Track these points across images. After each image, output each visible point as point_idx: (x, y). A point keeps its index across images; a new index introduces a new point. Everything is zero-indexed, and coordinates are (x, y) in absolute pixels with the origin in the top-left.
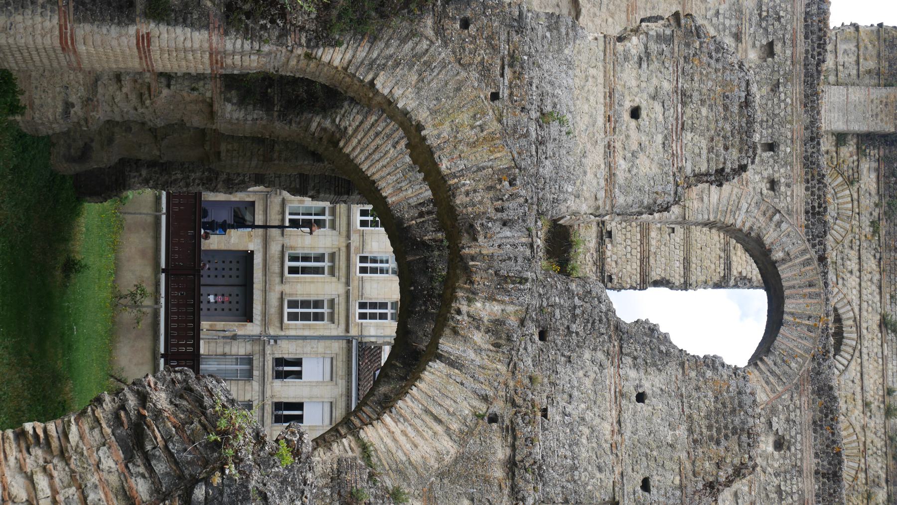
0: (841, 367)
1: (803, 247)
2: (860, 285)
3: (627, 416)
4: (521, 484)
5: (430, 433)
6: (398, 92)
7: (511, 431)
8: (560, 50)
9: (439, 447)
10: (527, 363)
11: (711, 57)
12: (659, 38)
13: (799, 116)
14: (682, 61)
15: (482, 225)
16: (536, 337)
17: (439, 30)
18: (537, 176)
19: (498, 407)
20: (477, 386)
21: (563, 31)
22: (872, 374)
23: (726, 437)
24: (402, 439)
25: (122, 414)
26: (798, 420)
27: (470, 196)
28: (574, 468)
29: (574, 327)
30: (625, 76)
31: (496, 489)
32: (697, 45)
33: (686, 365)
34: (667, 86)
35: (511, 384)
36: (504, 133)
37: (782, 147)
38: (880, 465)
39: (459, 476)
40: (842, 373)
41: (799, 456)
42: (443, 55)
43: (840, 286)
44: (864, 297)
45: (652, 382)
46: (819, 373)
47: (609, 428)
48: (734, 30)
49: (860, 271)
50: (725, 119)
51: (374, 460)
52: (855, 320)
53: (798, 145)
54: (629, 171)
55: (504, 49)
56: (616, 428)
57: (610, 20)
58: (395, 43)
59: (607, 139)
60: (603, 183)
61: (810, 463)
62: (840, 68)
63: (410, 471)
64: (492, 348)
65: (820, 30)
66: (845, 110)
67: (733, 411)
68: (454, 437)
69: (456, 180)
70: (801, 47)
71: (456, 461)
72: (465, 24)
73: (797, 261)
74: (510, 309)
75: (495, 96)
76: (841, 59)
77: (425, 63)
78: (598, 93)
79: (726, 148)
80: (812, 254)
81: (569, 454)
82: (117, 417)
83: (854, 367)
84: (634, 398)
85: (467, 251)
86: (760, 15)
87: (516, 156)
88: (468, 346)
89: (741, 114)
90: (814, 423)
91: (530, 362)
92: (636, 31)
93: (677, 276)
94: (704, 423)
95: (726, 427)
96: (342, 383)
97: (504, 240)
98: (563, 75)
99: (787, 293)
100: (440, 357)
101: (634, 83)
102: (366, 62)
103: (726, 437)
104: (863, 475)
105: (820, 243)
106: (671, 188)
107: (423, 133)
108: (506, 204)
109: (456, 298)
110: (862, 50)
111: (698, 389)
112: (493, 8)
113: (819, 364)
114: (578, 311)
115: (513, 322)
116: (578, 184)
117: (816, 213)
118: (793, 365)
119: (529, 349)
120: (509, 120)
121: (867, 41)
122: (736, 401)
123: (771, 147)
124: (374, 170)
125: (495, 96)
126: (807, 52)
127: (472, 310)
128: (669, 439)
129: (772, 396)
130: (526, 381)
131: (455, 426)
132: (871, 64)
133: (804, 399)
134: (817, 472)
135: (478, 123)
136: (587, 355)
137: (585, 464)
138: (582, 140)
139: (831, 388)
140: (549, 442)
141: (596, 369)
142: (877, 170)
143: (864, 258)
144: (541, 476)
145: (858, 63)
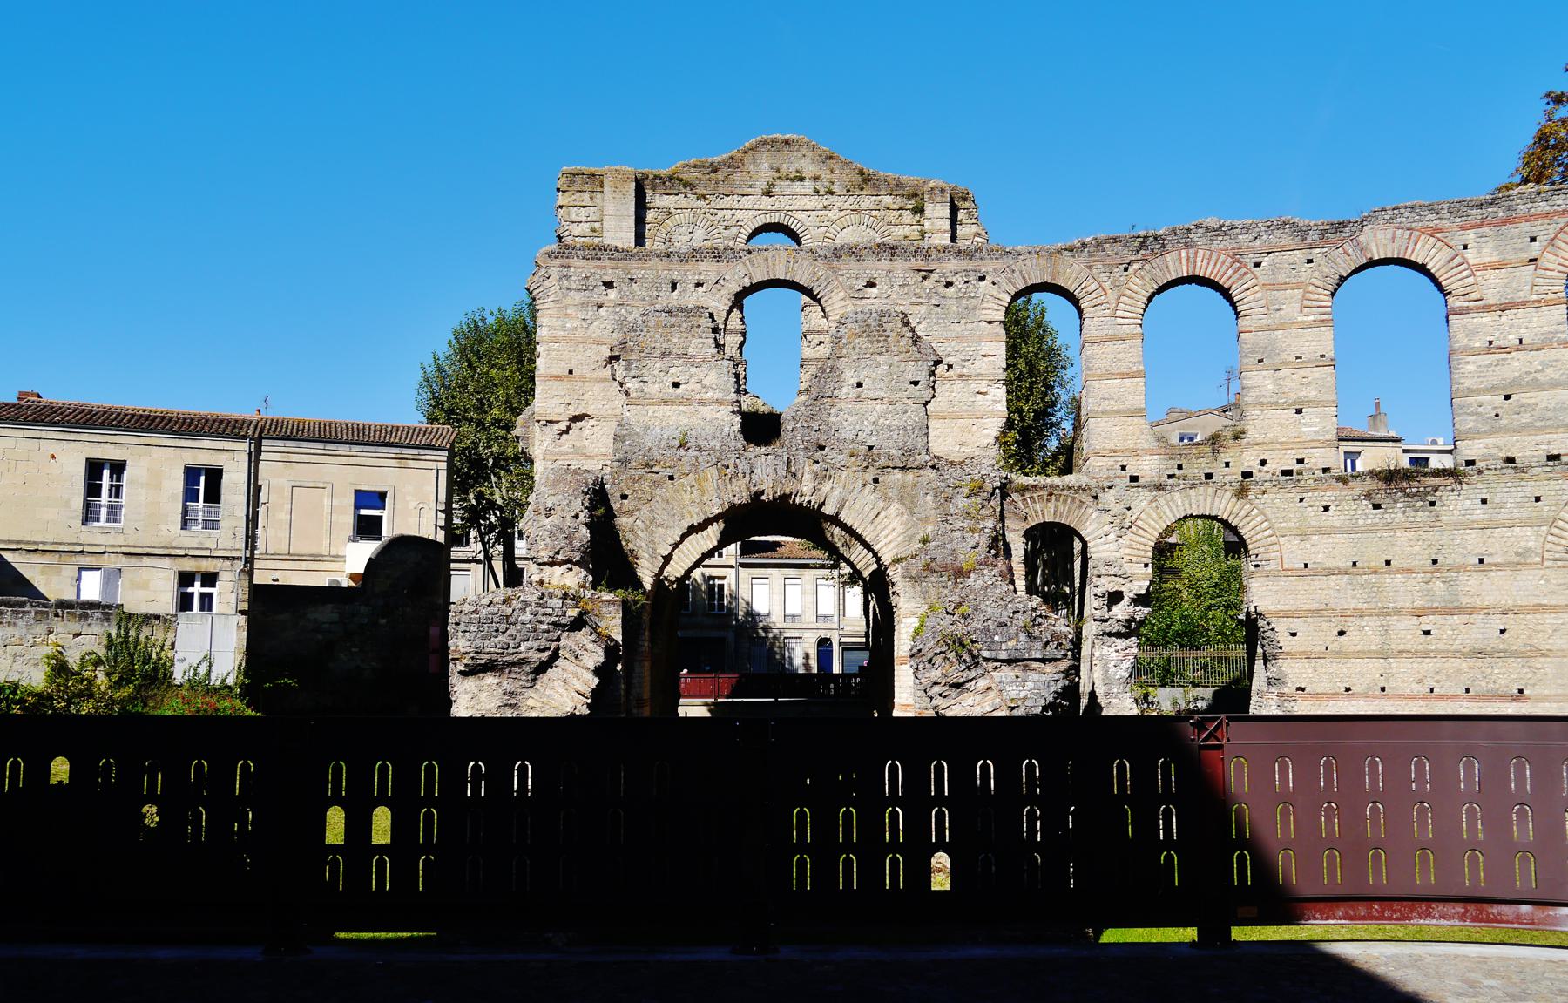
3: (871, 395)
10: (842, 458)
12: (628, 369)
17: (629, 513)
19: (869, 477)
28: (905, 429)
45: (850, 378)
53: (673, 266)
70: (606, 262)
72: (624, 497)
74: (807, 469)
75: (671, 478)
83: (799, 215)
92: (621, 384)
117: (718, 255)
120: (687, 469)
125: (671, 478)
132: (586, 196)
136: (833, 419)
138: (695, 421)
140: (889, 444)
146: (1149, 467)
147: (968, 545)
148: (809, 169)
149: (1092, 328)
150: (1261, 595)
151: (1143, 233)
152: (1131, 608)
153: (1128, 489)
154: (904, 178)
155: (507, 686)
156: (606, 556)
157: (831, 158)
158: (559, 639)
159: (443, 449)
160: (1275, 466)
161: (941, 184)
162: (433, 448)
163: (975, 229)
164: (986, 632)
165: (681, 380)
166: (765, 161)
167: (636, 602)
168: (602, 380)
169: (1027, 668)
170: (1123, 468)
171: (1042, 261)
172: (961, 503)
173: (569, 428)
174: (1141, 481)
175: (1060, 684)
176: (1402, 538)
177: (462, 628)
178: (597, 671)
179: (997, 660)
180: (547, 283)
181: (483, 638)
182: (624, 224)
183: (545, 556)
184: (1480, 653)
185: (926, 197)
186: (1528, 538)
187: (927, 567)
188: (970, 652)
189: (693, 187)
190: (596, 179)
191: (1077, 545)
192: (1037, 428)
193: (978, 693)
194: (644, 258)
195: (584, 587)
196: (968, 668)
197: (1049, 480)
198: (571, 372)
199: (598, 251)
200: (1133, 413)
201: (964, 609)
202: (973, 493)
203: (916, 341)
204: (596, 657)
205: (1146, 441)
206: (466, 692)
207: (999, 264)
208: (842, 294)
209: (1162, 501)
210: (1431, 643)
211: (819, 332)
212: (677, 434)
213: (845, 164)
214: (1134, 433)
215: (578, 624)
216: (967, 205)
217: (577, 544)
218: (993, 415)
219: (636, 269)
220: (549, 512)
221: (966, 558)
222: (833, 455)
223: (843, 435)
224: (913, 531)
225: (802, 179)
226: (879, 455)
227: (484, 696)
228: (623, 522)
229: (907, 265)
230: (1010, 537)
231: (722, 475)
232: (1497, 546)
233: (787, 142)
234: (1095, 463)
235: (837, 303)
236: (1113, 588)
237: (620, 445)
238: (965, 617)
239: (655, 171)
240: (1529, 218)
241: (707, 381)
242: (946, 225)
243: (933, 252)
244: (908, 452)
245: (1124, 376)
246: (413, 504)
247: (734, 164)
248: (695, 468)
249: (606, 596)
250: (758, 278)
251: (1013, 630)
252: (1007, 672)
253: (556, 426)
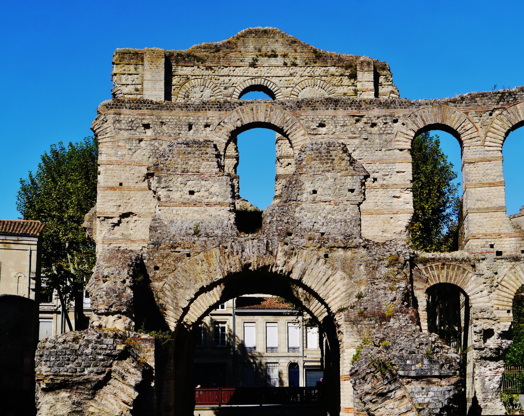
0: (274, 86)
1: (236, 112)
2: (235, 76)
3: (323, 199)
4: (353, 244)
5: (333, 283)
6: (188, 298)
7: (331, 248)
8: (166, 226)
9: (339, 278)
10: (303, 241)
11: (167, 159)
12: (159, 182)
13: (176, 113)
14: (169, 172)
15: (245, 260)
16: (291, 237)
17: (160, 279)
18: (222, 237)
19: (322, 253)
20: (313, 263)
21: (157, 225)
22: (276, 72)
23: (331, 156)
24: (336, 295)
25: (373, 401)
26: (312, 117)
28: (345, 221)
29: (286, 221)
30: (176, 197)
31: (356, 255)
32: (162, 165)
33: (301, 173)
34: (180, 179)
35: (312, 248)
36: (205, 251)
37: (191, 121)
38: (318, 70)
39: (351, 270)
40: (276, 86)
41: (328, 117)
42: (171, 278)
43: (236, 85)
44: (241, 74)
45: (308, 187)
46: (291, 107)
47: (328, 206)
48: (138, 142)
49: (229, 76)
50: (194, 153)
51: (345, 307)
52: (252, 79)
54: (218, 196)
55: (168, 251)
56: (328, 203)
57: (134, 198)
58: (166, 299)
59: (204, 205)
60: (223, 208)
61: (331, 112)
62: (134, 83)
63: (349, 291)
64: (296, 256)
65: (137, 102)
67: (320, 153)
68: (334, 273)
69: (225, 272)
70: (145, 111)
71: (345, 272)
72: (157, 268)
73: (241, 115)
74: (280, 248)
75: (188, 255)
76: (130, 83)
77: (175, 286)
78: (184, 209)
79: (207, 153)
80: (238, 108)
81: (340, 224)
82: (374, 403)
83: (274, 80)
84: (315, 195)
85: (256, 267)
86: (131, 130)
87: (214, 246)
89: (192, 147)
90: (313, 110)
91: (302, 240)
92: (155, 192)
93: (232, 162)
94: (325, 165)
95: (327, 156)
96: (256, 317)
97: (251, 251)
98: (177, 224)
99: (256, 120)
100: (301, 279)
101: (179, 194)
102: (175, 311)
103: (331, 156)
104: (323, 78)
105: (234, 105)
106: (225, 178)
107: (205, 286)
108: (235, 250)
109: (276, 272)
110: (125, 72)
111: (311, 168)
112: (150, 256)
113: (287, 107)
114: (279, 219)
115: (286, 247)
116: (223, 218)
117: (220, 106)
118: (288, 118)
119: (296, 241)
120: (199, 249)
121: (121, 70)
122: (316, 151)
124: (205, 306)
125: (188, 255)
126: (147, 109)
127: (281, 265)
128: (333, 180)
129: (302, 128)
130: (311, 242)
131: (330, 272)
132: (132, 67)
133: (303, 114)
134: (335, 109)
135: (201, 263)
136: (297, 215)
137: (343, 216)
138: (205, 216)
139: (298, 102)
140: (335, 231)
141: (303, 211)
142: (182, 66)
143: (223, 74)
144: (349, 236)
145: (131, 74)
147: (388, 299)
148: (280, 49)
149: (469, 154)
151: (501, 90)
152: (499, 341)
153: (495, 260)
154: (343, 55)
156: (144, 308)
157: (294, 42)
158: (111, 366)
159: (35, 236)
161: (368, 59)
162: (28, 236)
163: (390, 88)
164: (401, 358)
165: (195, 189)
166: (251, 44)
167: (164, 340)
168: (142, 190)
169: (429, 382)
170: (492, 246)
171: (435, 110)
172: (384, 271)
173: (120, 222)
174: (504, 255)
175: (452, 393)
177: (44, 358)
178: (137, 388)
179: (409, 377)
180: (105, 125)
181: (59, 365)
182: (157, 86)
183: (102, 308)
185: (358, 68)
187: (361, 314)
188: (391, 372)
189: (203, 61)
190: (138, 57)
191: (462, 298)
193: (396, 400)
195: (129, 329)
196: (390, 383)
197: (442, 255)
198: (121, 184)
199: (139, 104)
200: (497, 209)
201: (387, 342)
202: (391, 264)
203: (352, 162)
204: (135, 377)
205: (507, 228)
207: (407, 112)
208: (302, 132)
209: (518, 268)
211: (288, 157)
212: (192, 225)
213: (306, 46)
214: (499, 222)
215: (123, 356)
216: (385, 72)
217: (124, 300)
218: (404, 212)
219: (165, 115)
220: (105, 279)
221: (387, 307)
222: (297, 239)
223: (304, 225)
224: (352, 290)
225: (276, 56)
226: (328, 239)
227: (59, 405)
228: (156, 285)
229: (346, 112)
230: (417, 293)
231: (223, 253)
233: (265, 32)
234: (472, 243)
236: (486, 327)
237: (154, 233)
238: (387, 348)
239: (178, 51)
241: (212, 190)
242: (371, 86)
243: (363, 104)
244: (348, 237)
245: (491, 185)
246: (13, 274)
247: (230, 46)
248: (204, 248)
249: (144, 336)
250: (246, 121)
251: (419, 356)
252: (416, 386)
253: (111, 221)
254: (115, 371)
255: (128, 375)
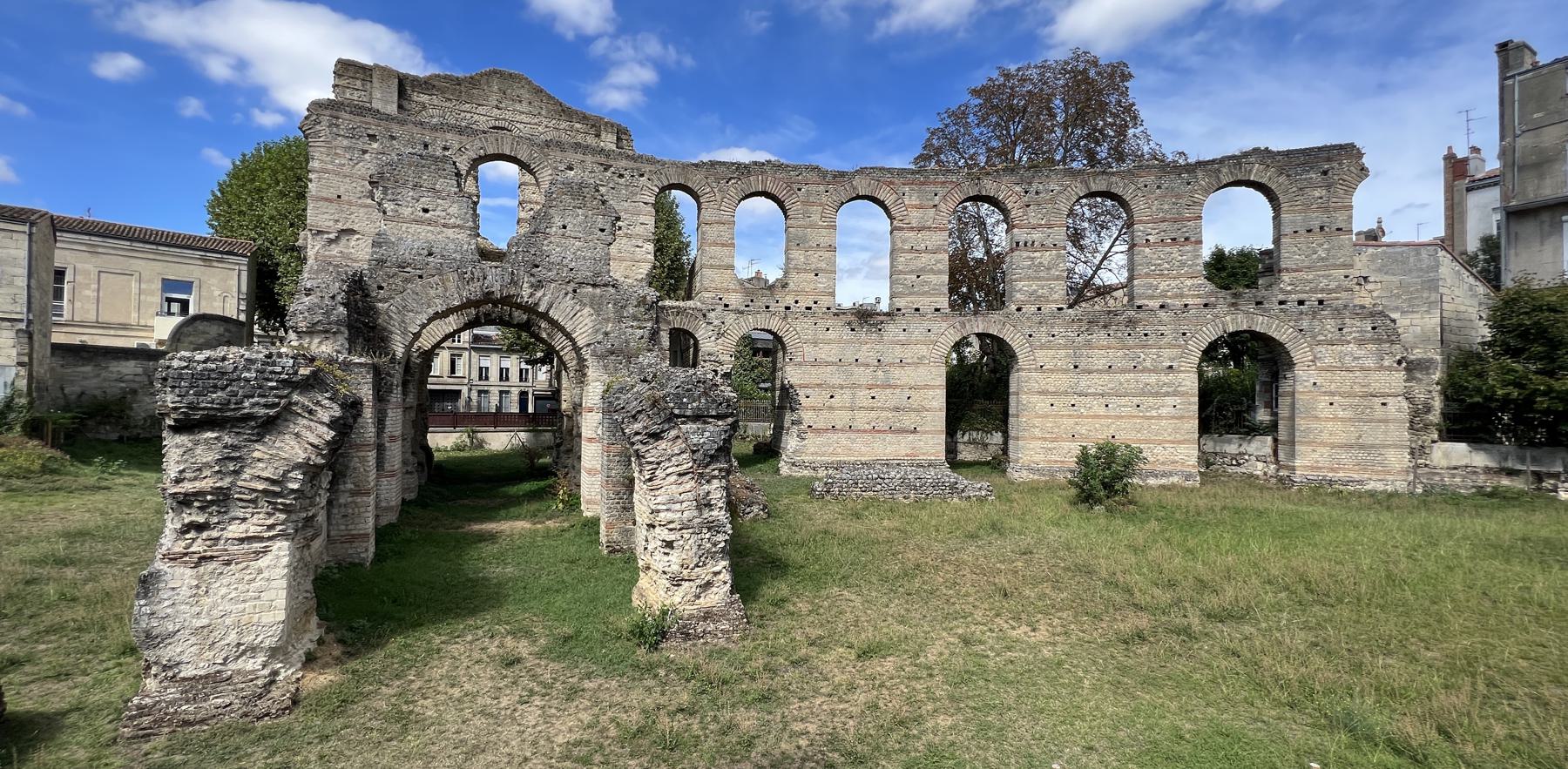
12: (385, 193)
17: (384, 300)
19: (570, 289)
27: (474, 290)
45: (558, 221)
61: (580, 156)
66: (387, 102)
72: (381, 288)
78: (414, 227)
88: (543, 299)
92: (380, 204)
123: (426, 146)
146: (735, 299)
147: (636, 334)
150: (792, 375)
155: (227, 439)
160: (803, 304)
165: (430, 207)
168: (367, 206)
169: (705, 422)
176: (865, 348)
178: (332, 425)
183: (303, 325)
184: (897, 409)
186: (923, 350)
192: (674, 273)
194: (402, 123)
206: (177, 446)
207: (653, 168)
210: (875, 403)
218: (645, 261)
219: (396, 130)
220: (309, 292)
232: (909, 354)
235: (546, 176)
240: (934, 183)
241: (450, 211)
244: (598, 274)
245: (723, 245)
246: (217, 293)
247: (473, 82)
250: (491, 151)
254: (296, 404)
255: (318, 408)
